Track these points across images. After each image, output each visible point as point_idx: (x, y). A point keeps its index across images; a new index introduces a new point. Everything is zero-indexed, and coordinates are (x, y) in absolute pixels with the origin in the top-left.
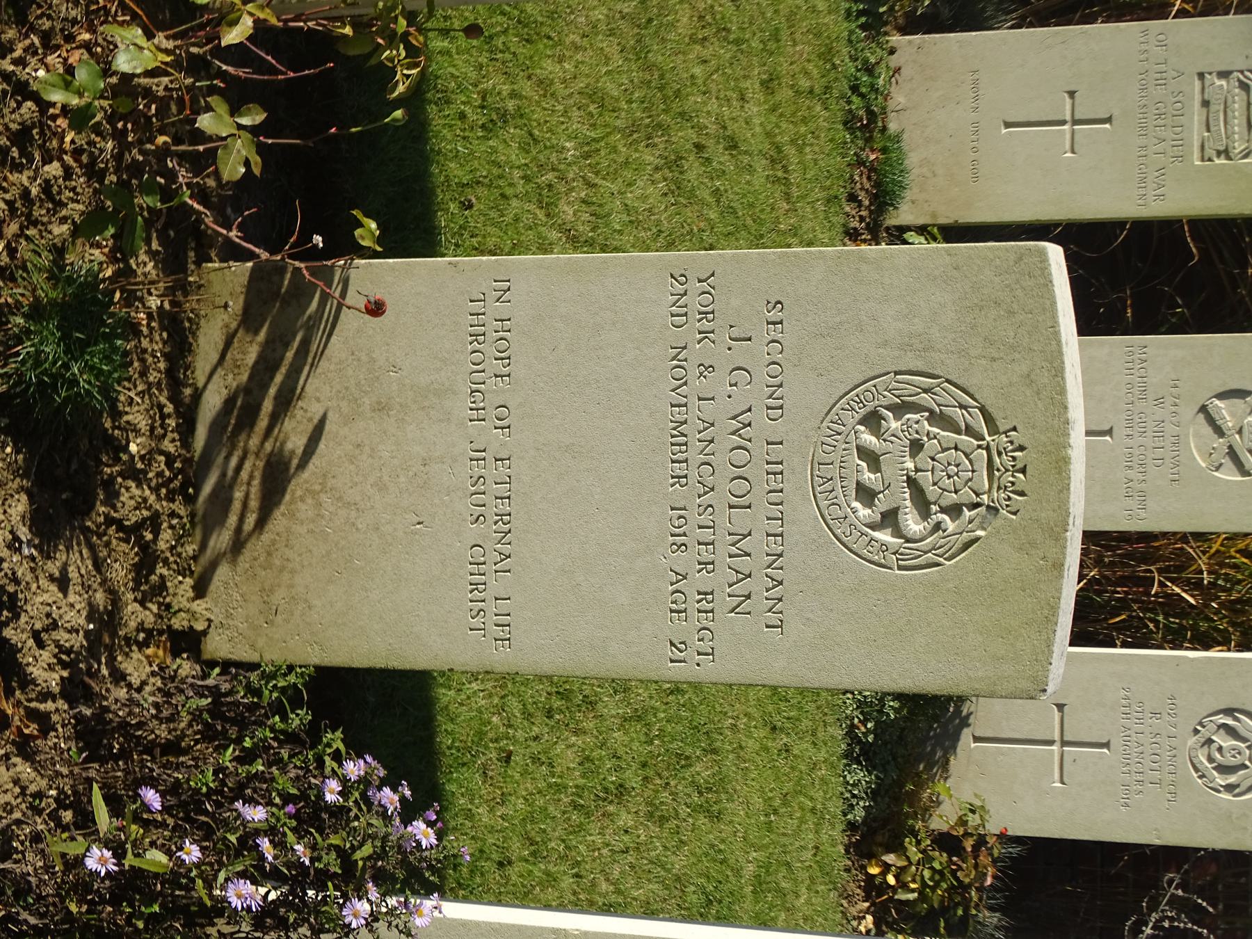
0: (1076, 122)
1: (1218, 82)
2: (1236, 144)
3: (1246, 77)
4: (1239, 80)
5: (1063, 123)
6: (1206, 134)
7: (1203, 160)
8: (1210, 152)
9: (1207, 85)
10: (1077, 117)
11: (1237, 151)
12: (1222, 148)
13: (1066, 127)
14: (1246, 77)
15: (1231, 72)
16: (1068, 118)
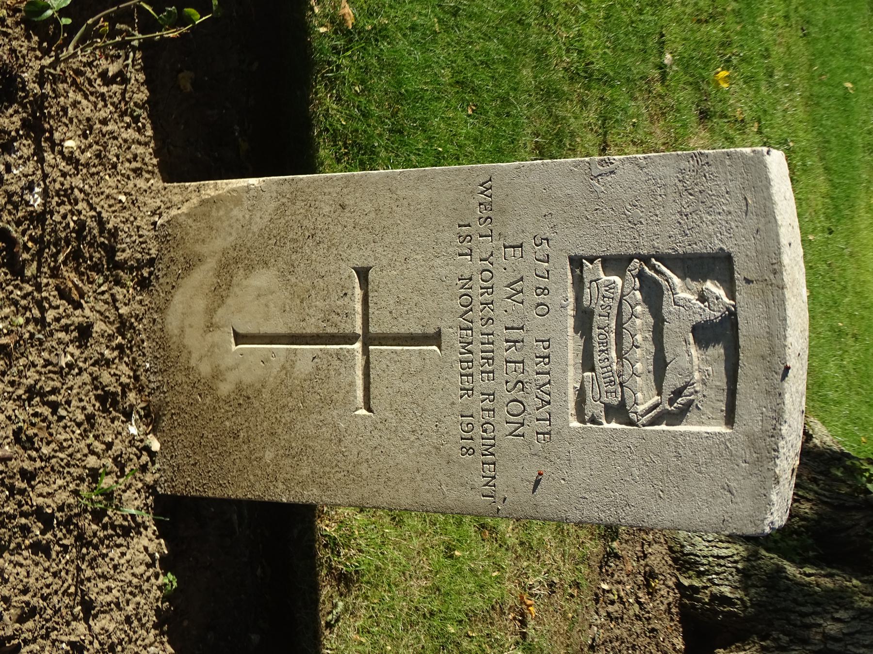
0: (369, 340)
1: (604, 278)
2: (639, 395)
3: (653, 268)
4: (641, 275)
5: (350, 339)
6: (588, 374)
7: (583, 421)
8: (594, 408)
9: (587, 277)
10: (373, 329)
11: (641, 408)
12: (615, 401)
13: (358, 346)
14: (653, 268)
15: (630, 259)
16: (359, 331)
